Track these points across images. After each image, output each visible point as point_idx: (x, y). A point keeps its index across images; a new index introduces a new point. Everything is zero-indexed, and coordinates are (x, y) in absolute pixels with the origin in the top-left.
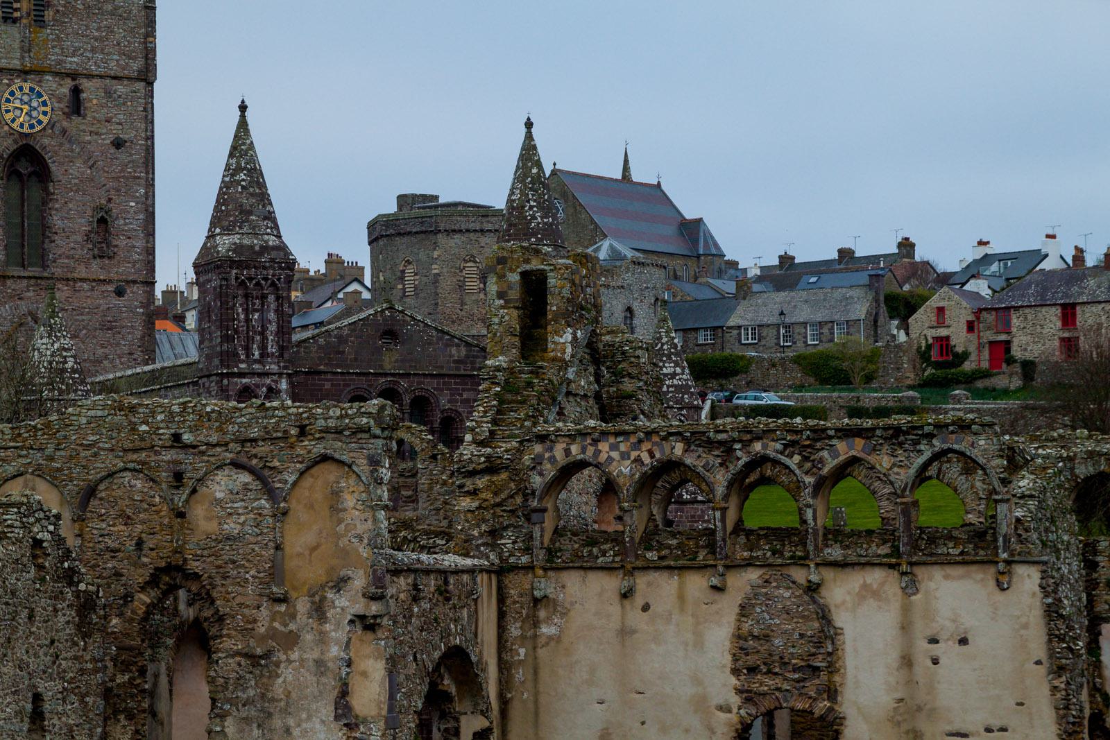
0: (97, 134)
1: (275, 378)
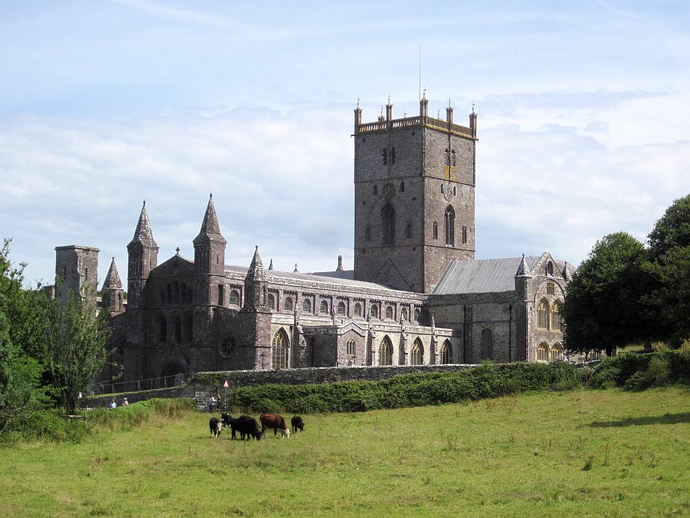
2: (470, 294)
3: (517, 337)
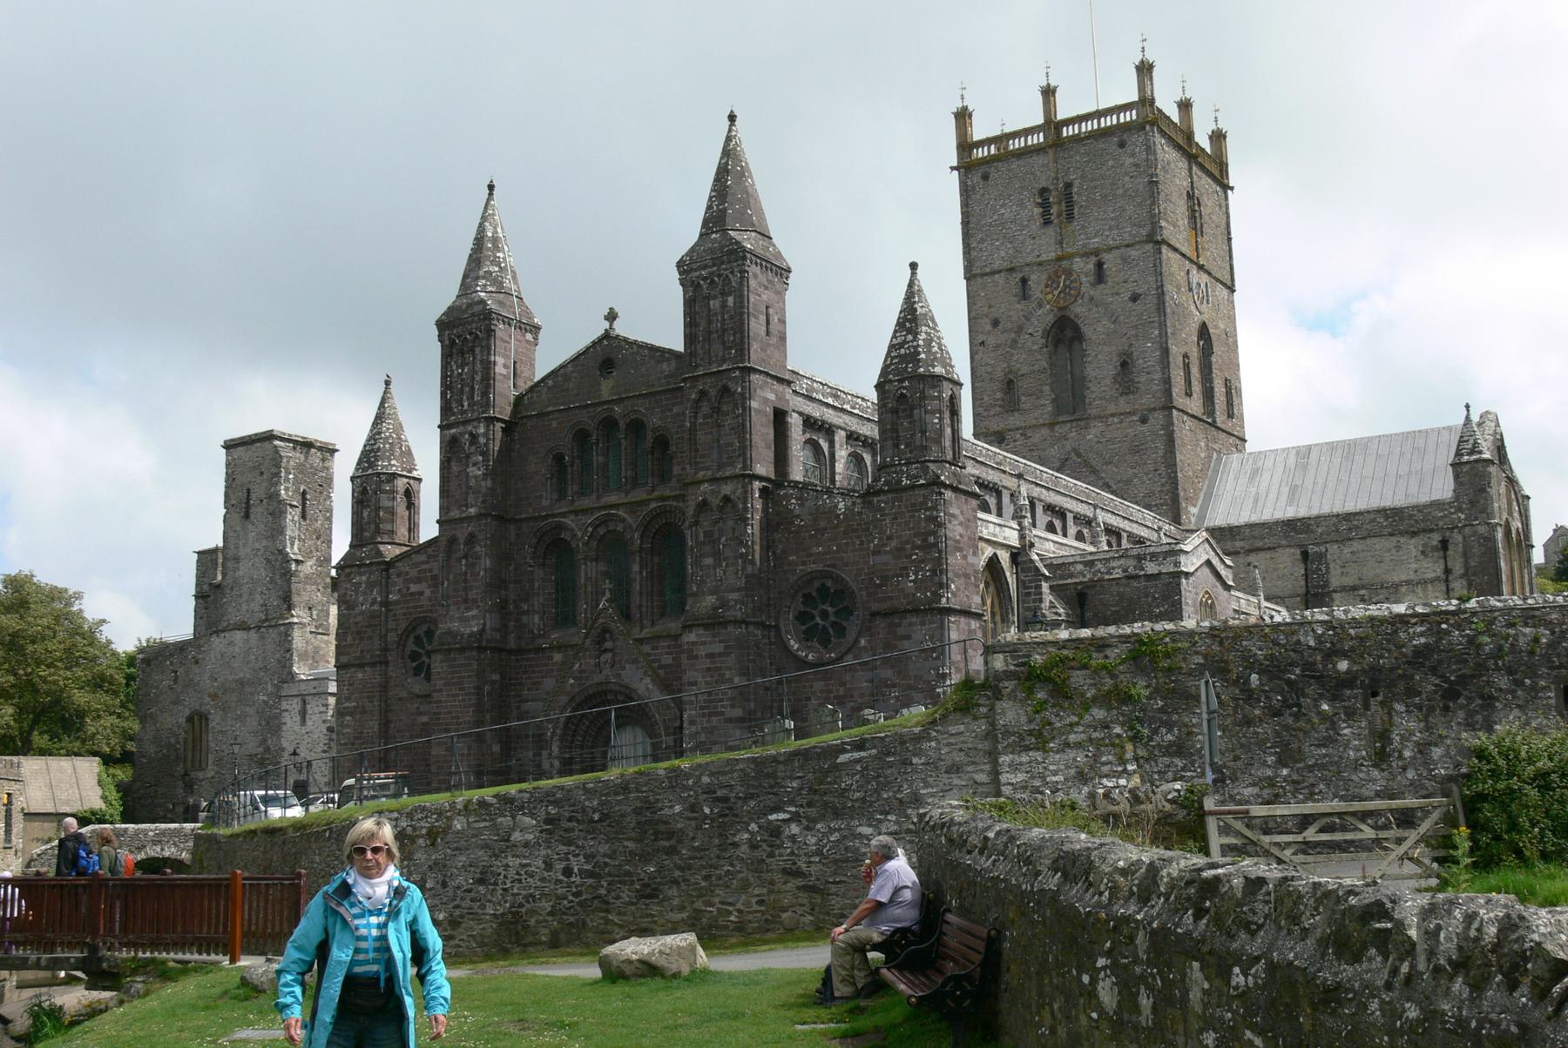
0: (1118, 294)
1: (475, 424)
2: (1318, 519)
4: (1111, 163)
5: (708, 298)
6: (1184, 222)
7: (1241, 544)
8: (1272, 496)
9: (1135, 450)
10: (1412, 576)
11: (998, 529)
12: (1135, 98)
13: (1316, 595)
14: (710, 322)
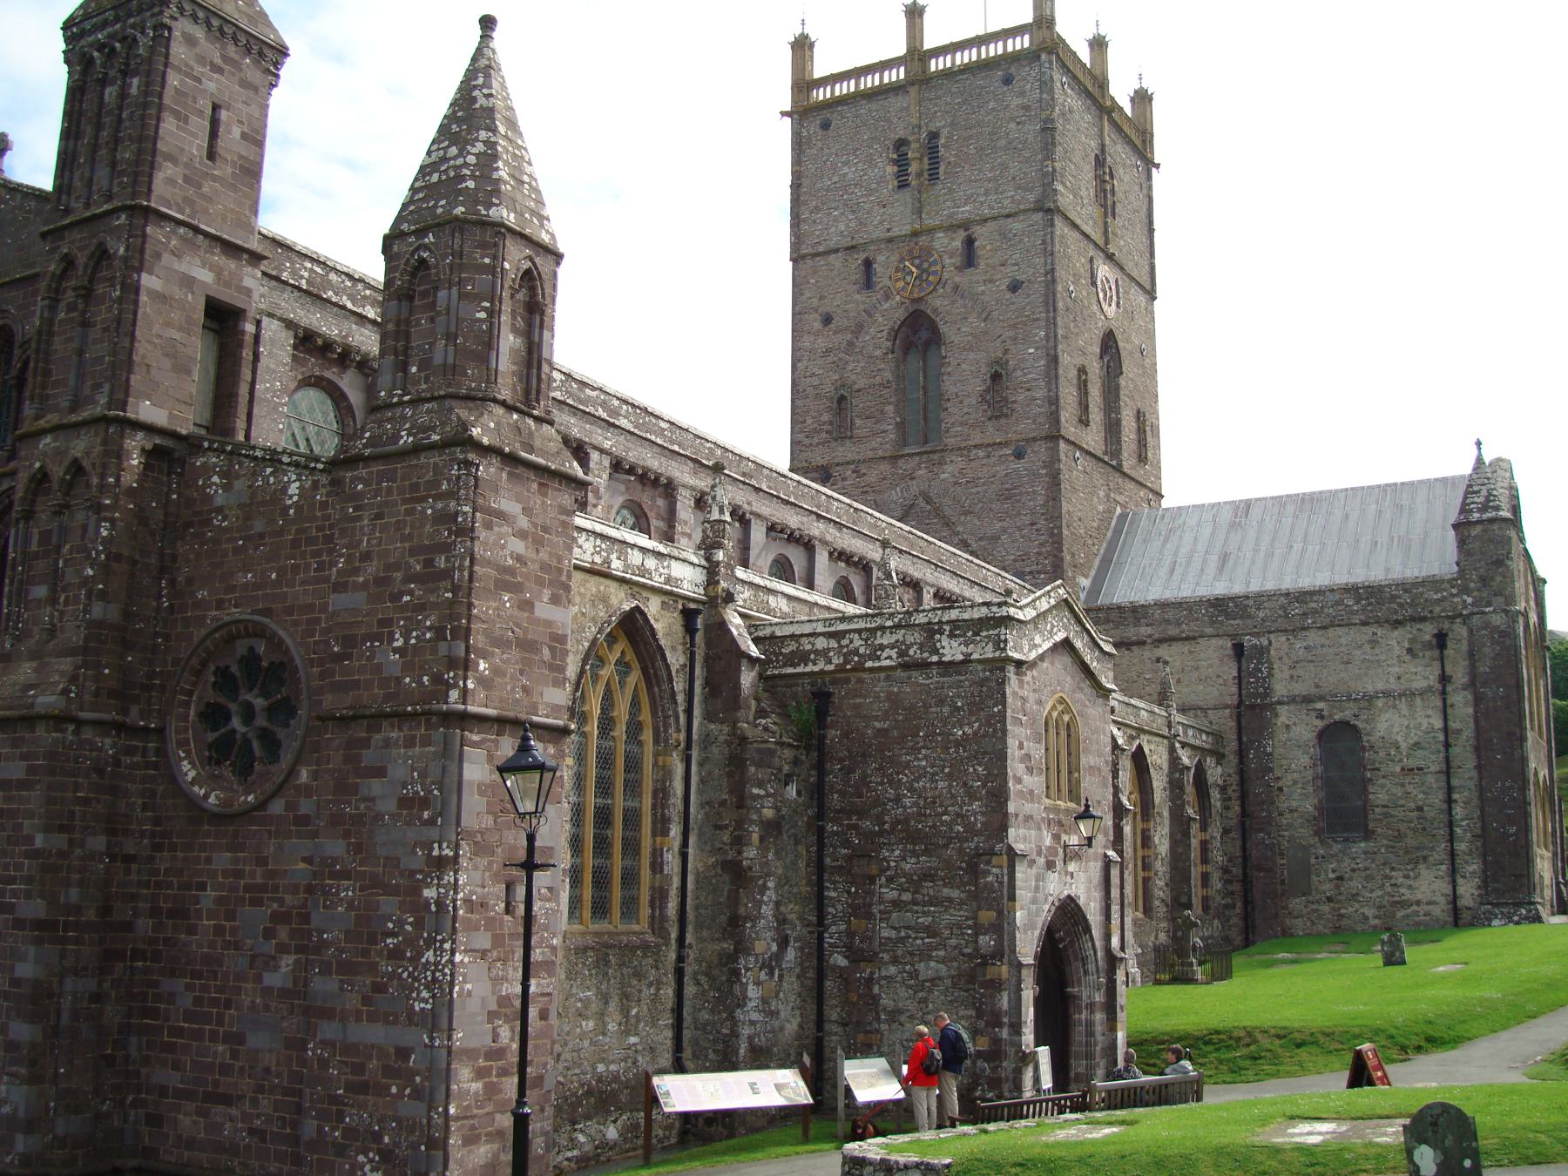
0: (992, 281)
2: (1260, 598)
3: (1480, 748)
4: (991, 105)
5: (104, 82)
6: (1088, 191)
7: (1149, 630)
8: (1196, 564)
9: (1007, 496)
10: (1393, 685)
11: (651, 563)
12: (1028, 17)
13: (1253, 707)
14: (99, 127)
